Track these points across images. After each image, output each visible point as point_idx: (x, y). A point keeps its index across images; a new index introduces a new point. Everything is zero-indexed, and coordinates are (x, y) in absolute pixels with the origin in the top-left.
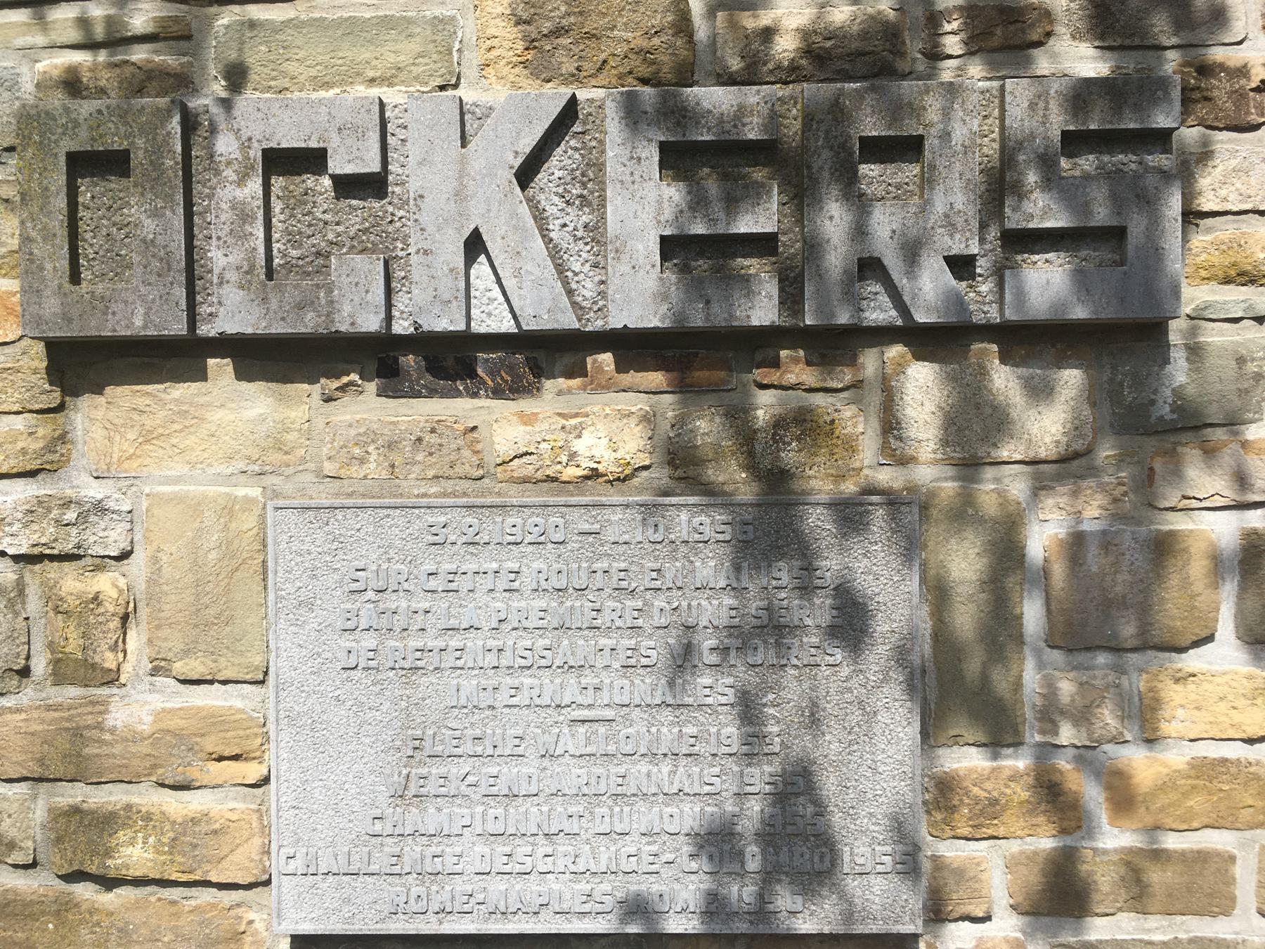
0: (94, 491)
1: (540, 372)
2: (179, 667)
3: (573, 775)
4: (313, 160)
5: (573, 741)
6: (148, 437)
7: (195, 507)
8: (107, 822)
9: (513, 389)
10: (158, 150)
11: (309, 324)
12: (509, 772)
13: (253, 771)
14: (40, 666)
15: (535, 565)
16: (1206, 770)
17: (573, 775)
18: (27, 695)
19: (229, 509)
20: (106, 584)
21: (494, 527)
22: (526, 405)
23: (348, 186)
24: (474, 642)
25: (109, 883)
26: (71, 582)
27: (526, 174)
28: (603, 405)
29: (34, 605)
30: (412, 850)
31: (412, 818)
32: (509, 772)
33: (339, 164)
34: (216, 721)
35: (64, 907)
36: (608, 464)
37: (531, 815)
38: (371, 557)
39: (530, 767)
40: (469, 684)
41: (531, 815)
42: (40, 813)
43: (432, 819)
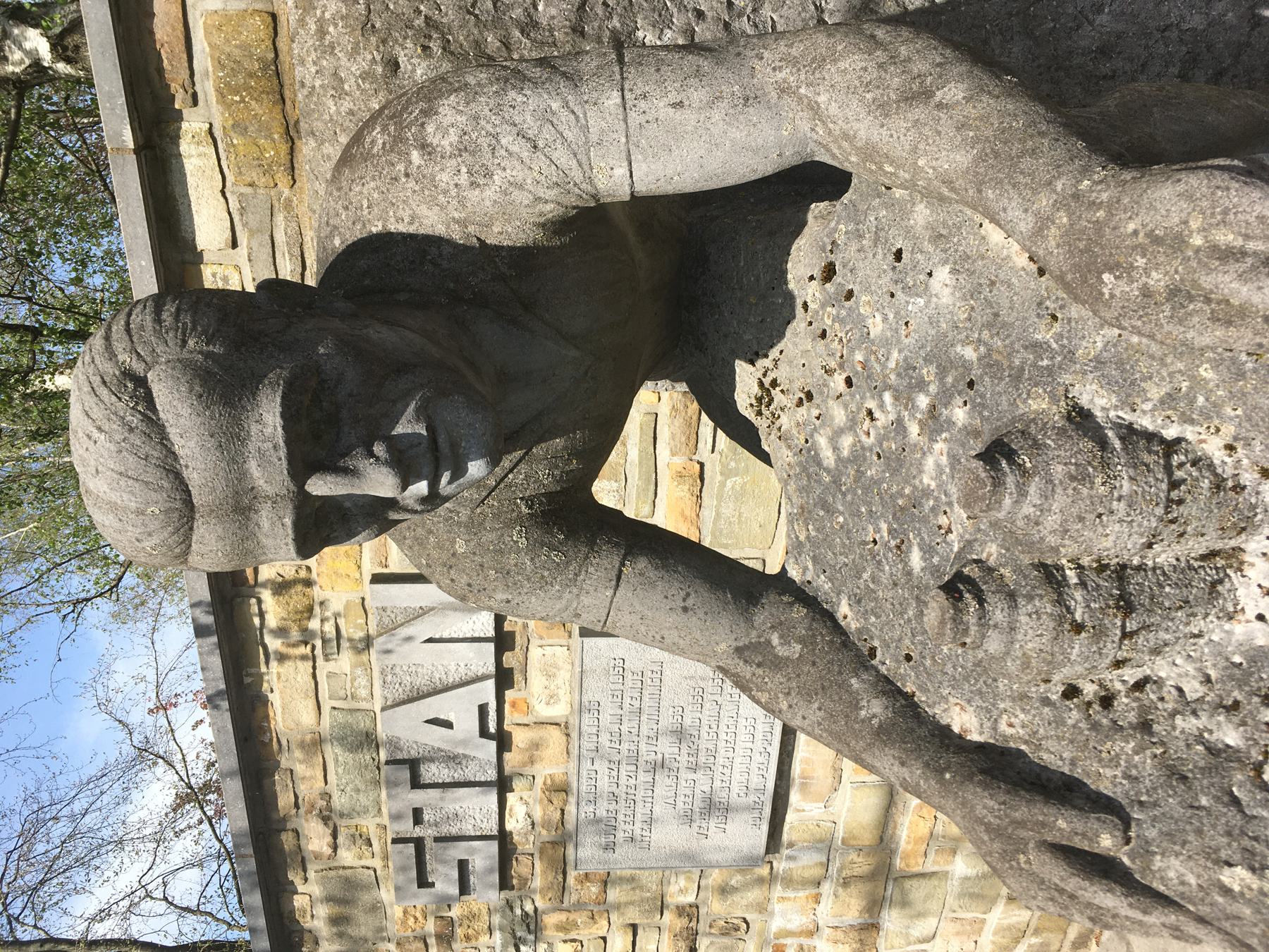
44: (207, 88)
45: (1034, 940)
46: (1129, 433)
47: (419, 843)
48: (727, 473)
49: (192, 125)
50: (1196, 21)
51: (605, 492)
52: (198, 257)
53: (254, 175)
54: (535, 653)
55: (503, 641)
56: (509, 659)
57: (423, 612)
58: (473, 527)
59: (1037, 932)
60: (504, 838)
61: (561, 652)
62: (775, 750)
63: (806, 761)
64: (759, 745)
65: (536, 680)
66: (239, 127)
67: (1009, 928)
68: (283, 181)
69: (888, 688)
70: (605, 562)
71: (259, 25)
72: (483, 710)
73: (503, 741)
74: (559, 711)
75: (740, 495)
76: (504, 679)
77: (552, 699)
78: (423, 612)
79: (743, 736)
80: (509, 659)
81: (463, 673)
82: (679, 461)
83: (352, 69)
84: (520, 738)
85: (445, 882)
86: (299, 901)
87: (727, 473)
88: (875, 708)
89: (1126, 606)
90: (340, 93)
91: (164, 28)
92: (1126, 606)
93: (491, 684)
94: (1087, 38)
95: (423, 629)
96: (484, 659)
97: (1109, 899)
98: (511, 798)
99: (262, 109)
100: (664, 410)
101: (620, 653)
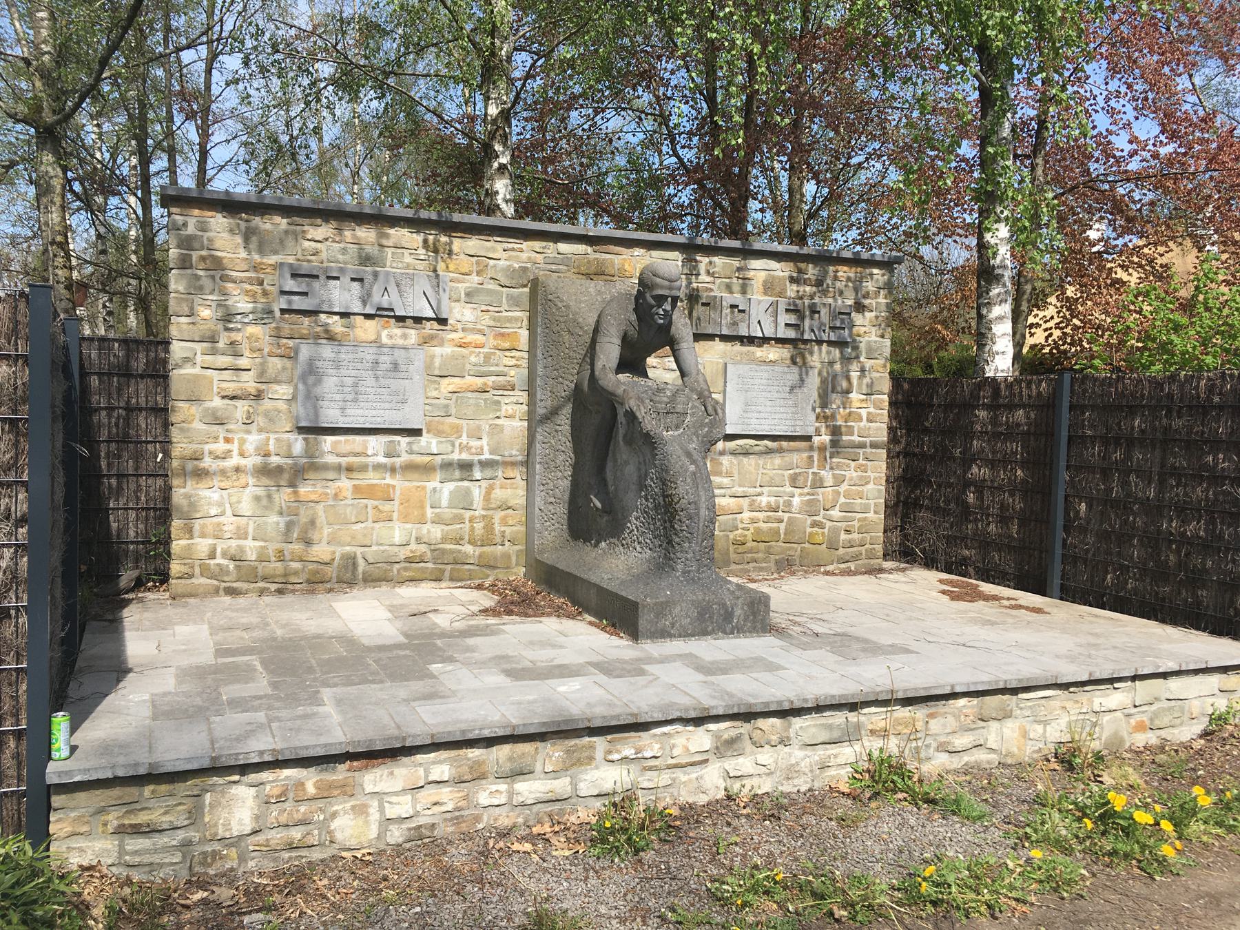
3: (769, 409)
5: (769, 403)
9: (760, 346)
15: (765, 375)
17: (769, 409)
21: (758, 368)
23: (740, 311)
28: (773, 349)
32: (760, 408)
43: (749, 415)
44: (598, 255)
45: (231, 567)
48: (485, 400)
49: (589, 249)
54: (413, 332)
55: (418, 320)
56: (409, 322)
59: (237, 567)
61: (413, 341)
62: (367, 426)
63: (354, 442)
65: (398, 332)
66: (589, 262)
75: (477, 405)
79: (374, 412)
80: (409, 322)
82: (490, 383)
86: (278, 219)
87: (485, 400)
93: (403, 314)
98: (336, 318)
99: (593, 269)
100: (508, 378)
101: (416, 363)
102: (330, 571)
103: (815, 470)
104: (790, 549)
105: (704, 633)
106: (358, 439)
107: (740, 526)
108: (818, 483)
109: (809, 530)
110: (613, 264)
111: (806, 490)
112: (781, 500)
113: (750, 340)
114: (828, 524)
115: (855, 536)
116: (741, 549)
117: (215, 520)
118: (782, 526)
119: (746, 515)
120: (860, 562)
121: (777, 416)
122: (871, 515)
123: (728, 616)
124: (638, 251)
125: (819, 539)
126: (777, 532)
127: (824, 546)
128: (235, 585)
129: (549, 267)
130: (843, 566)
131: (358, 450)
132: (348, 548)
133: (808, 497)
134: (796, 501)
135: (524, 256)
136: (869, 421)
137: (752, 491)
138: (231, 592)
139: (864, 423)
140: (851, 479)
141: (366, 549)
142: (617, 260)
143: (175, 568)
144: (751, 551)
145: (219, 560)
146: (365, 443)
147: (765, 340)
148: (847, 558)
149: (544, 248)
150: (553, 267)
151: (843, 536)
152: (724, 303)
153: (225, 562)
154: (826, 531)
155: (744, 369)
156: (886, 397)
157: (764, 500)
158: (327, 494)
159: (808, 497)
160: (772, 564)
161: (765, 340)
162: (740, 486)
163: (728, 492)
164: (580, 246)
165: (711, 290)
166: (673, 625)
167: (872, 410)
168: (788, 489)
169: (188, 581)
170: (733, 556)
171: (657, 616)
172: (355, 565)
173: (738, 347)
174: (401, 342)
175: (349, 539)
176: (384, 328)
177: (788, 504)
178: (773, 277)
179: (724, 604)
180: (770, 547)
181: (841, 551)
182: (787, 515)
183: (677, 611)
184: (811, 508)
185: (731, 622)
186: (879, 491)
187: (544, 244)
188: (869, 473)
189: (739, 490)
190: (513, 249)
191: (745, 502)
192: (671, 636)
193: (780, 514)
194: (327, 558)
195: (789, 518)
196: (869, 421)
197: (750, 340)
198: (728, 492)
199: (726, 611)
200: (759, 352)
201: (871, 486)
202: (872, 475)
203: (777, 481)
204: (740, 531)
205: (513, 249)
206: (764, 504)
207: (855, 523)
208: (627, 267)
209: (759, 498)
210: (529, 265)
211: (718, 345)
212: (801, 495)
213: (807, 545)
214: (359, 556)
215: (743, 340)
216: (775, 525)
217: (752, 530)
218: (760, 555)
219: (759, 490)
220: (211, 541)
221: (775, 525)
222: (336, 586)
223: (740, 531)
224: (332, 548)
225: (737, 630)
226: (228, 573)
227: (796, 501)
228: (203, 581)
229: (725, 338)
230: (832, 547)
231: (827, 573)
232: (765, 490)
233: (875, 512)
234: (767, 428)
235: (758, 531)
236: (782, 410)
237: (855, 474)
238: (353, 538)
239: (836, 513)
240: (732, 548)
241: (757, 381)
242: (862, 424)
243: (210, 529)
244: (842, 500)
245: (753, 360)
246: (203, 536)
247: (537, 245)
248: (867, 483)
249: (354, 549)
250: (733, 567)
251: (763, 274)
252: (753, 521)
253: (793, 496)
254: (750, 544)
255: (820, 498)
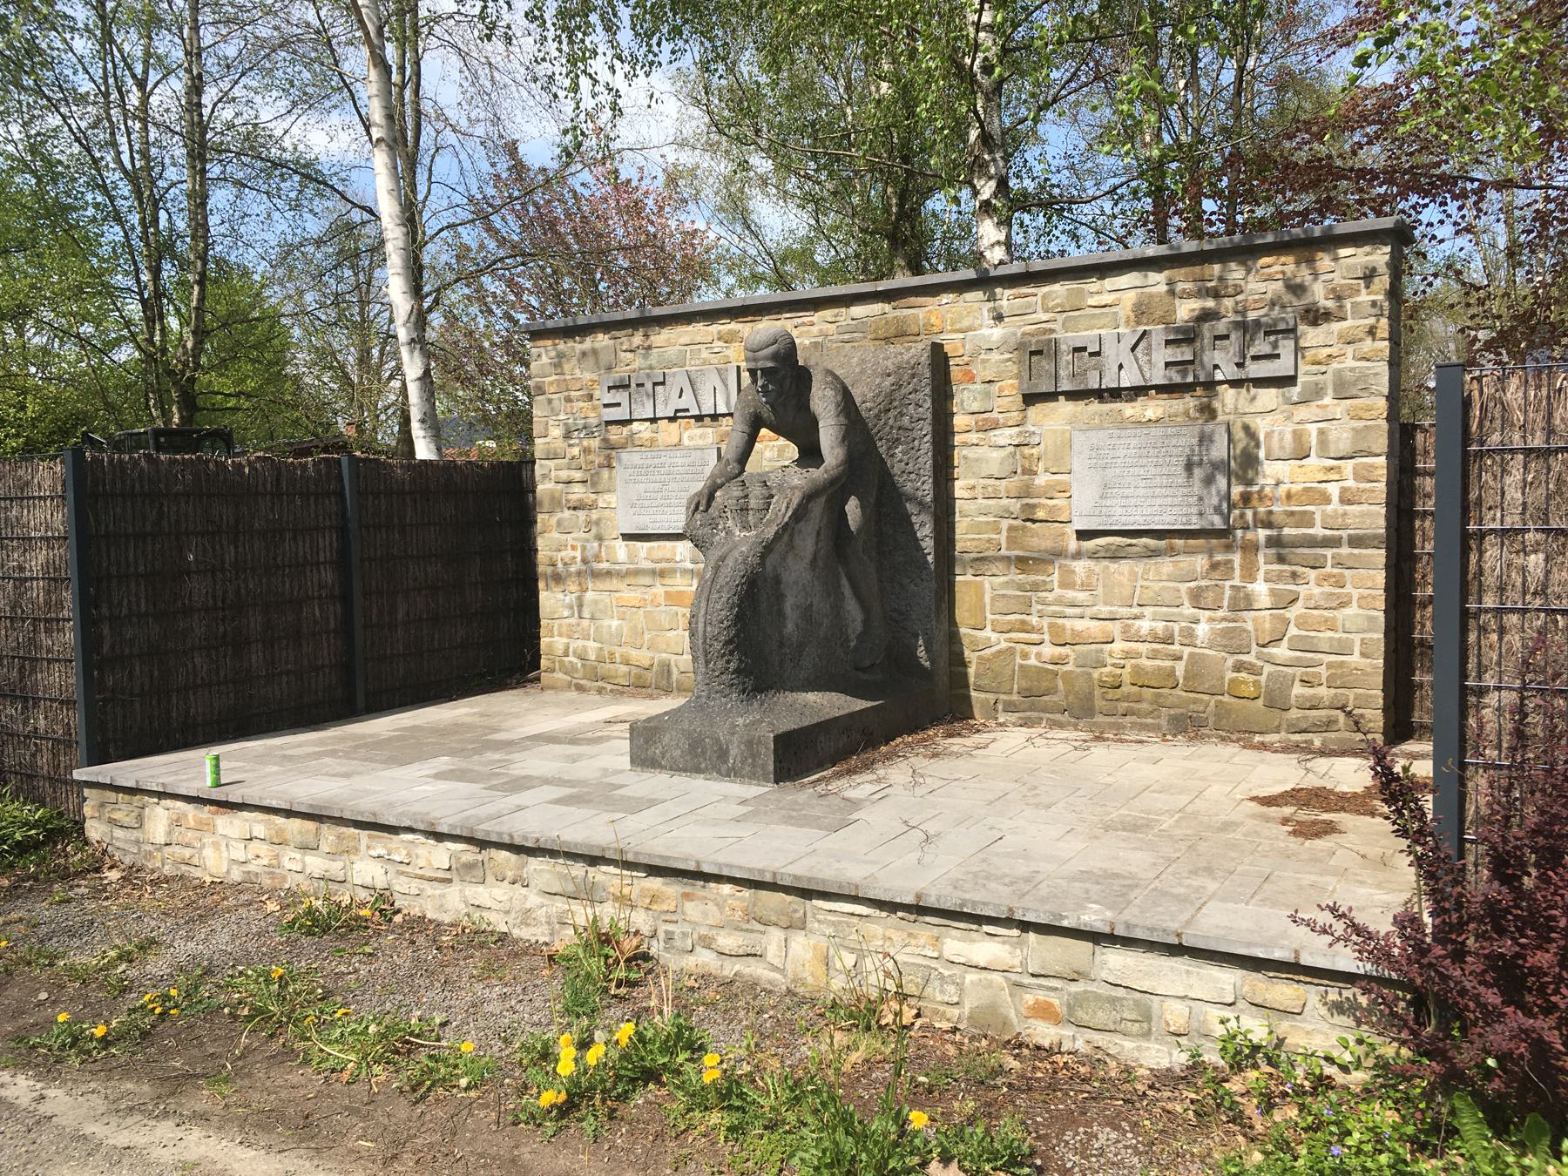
0: (1033, 429)
1: (1137, 396)
2: (1051, 470)
3: (1141, 492)
4: (1085, 349)
5: (1143, 484)
6: (1045, 416)
7: (1055, 432)
8: (1034, 506)
9: (1132, 400)
10: (1049, 349)
11: (1082, 387)
12: (1127, 492)
13: (1068, 495)
14: (1019, 471)
15: (1134, 442)
16: (1306, 490)
17: (1141, 492)
18: (1016, 478)
19: (1063, 432)
20: (1035, 451)
21: (1124, 433)
22: (1133, 404)
23: (1091, 354)
24: (1119, 461)
25: (1034, 521)
26: (1027, 451)
27: (1133, 349)
28: (1152, 403)
29: (1018, 456)
30: (1104, 510)
31: (1104, 502)
32: (1127, 492)
33: (1089, 350)
34: (1059, 483)
35: (1024, 527)
36: (1153, 418)
37: (1133, 501)
38: (1095, 441)
39: (1132, 490)
40: (1117, 471)
41: (1133, 501)
42: (1019, 506)
44: (898, 313)
46: (770, 504)
47: (628, 386)
49: (887, 307)
50: (914, 617)
51: (764, 431)
52: (848, 307)
53: (874, 327)
54: (710, 430)
55: (715, 417)
56: (707, 420)
57: (726, 386)
58: (754, 400)
59: (583, 665)
60: (630, 421)
62: (671, 531)
64: (673, 524)
65: (699, 431)
66: (887, 323)
67: (586, 651)
68: (873, 336)
69: (723, 485)
70: (747, 429)
71: (916, 330)
72: (687, 410)
73: (672, 419)
74: (686, 441)
76: (699, 418)
77: (691, 438)
78: (726, 386)
80: (707, 420)
81: (701, 401)
83: (889, 363)
84: (674, 426)
85: (609, 398)
86: (600, 336)
88: (719, 481)
89: (741, 510)
90: (884, 359)
91: (913, 300)
92: (741, 510)
94: (906, 581)
95: (720, 387)
96: (708, 409)
97: (693, 507)
98: (648, 424)
99: (892, 331)
102: (650, 677)
103: (1237, 582)
104: (1195, 701)
105: (697, 770)
106: (668, 544)
107: (1110, 661)
108: (1242, 603)
109: (1230, 675)
110: (916, 317)
111: (1220, 613)
112: (1176, 627)
113: (1116, 394)
114: (1268, 669)
115: (1322, 691)
116: (1111, 694)
117: (567, 621)
118: (1180, 668)
119: (1118, 646)
120: (1333, 735)
121: (1159, 501)
122: (1355, 659)
123: (723, 754)
124: (946, 298)
125: (1250, 690)
126: (1171, 673)
127: (1260, 702)
128: (582, 682)
129: (841, 337)
130: (1297, 737)
131: (669, 556)
132: (664, 655)
133: (1224, 625)
134: (1202, 630)
135: (815, 329)
136: (1344, 500)
137: (1125, 611)
138: (580, 689)
139: (1335, 506)
140: (1309, 597)
141: (679, 657)
142: (920, 313)
143: (543, 662)
144: (1127, 698)
145: (571, 658)
146: (674, 547)
147: (1138, 392)
148: (1304, 725)
149: (836, 316)
150: (846, 337)
151: (1298, 690)
152: (1063, 347)
153: (574, 660)
154: (1263, 679)
155: (1097, 437)
156: (1382, 460)
157: (1145, 626)
158: (645, 600)
159: (1224, 625)
160: (1164, 722)
161: (1138, 392)
162: (1106, 604)
163: (1089, 612)
164: (875, 306)
165: (1052, 331)
166: (663, 754)
167: (1351, 483)
168: (1188, 610)
169: (551, 675)
170: (1099, 703)
171: (646, 742)
172: (669, 672)
173: (1095, 406)
174: (701, 443)
175: (664, 647)
176: (686, 429)
177: (1189, 635)
178: (1151, 296)
179: (718, 740)
180: (1160, 695)
181: (1294, 713)
182: (1187, 651)
183: (666, 740)
184: (1232, 641)
185: (726, 762)
186: (1371, 619)
187: (836, 311)
188: (1348, 589)
189: (1104, 610)
190: (804, 324)
191: (1115, 628)
192: (662, 767)
193: (1176, 647)
194: (646, 663)
195: (1191, 655)
196: (1344, 500)
197: (1116, 394)
198: (1089, 612)
199: (721, 748)
200: (1129, 409)
201: (1352, 610)
202: (1356, 593)
203: (1167, 597)
204: (1109, 669)
205: (804, 324)
206: (1144, 631)
207: (1322, 670)
208: (933, 320)
209: (1137, 623)
210: (820, 340)
211: (1064, 407)
212: (1212, 620)
213: (1226, 698)
214: (673, 664)
215: (1100, 394)
216: (1168, 663)
217: (1128, 669)
218: (1144, 706)
219: (1136, 610)
220: (565, 640)
221: (1168, 663)
222: (655, 692)
223: (1109, 669)
224: (649, 654)
225: (732, 773)
226: (577, 670)
227: (1202, 630)
228: (561, 675)
229: (1073, 396)
230: (1276, 701)
231: (1263, 747)
232: (1148, 611)
233: (1363, 655)
234: (1141, 520)
235: (1137, 670)
236: (1169, 491)
237: (1317, 591)
238: (668, 645)
239: (1282, 652)
240: (1098, 692)
241: (1121, 452)
242: (1329, 508)
243: (564, 629)
244: (1293, 631)
245: (1122, 423)
246: (560, 635)
247: (828, 314)
248: (1343, 605)
249: (669, 656)
250: (1100, 719)
251: (1132, 294)
252: (1128, 655)
253: (1197, 622)
254: (1126, 689)
255: (1250, 626)
